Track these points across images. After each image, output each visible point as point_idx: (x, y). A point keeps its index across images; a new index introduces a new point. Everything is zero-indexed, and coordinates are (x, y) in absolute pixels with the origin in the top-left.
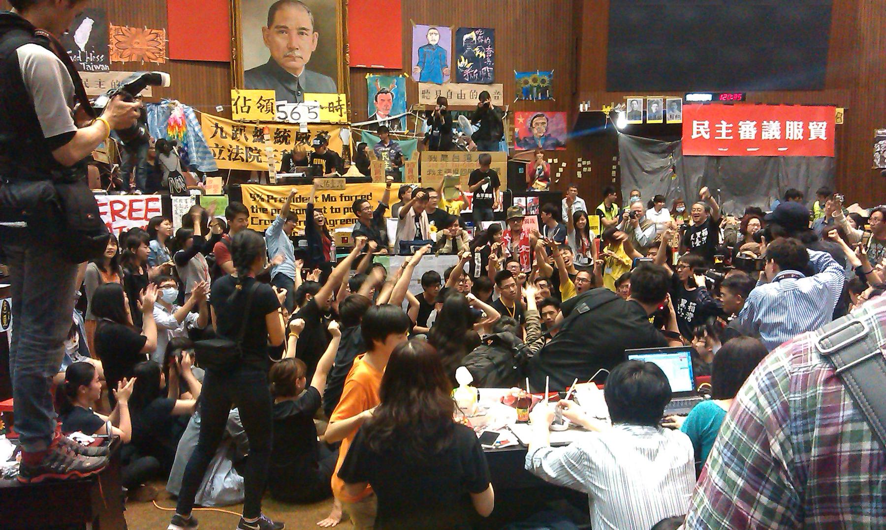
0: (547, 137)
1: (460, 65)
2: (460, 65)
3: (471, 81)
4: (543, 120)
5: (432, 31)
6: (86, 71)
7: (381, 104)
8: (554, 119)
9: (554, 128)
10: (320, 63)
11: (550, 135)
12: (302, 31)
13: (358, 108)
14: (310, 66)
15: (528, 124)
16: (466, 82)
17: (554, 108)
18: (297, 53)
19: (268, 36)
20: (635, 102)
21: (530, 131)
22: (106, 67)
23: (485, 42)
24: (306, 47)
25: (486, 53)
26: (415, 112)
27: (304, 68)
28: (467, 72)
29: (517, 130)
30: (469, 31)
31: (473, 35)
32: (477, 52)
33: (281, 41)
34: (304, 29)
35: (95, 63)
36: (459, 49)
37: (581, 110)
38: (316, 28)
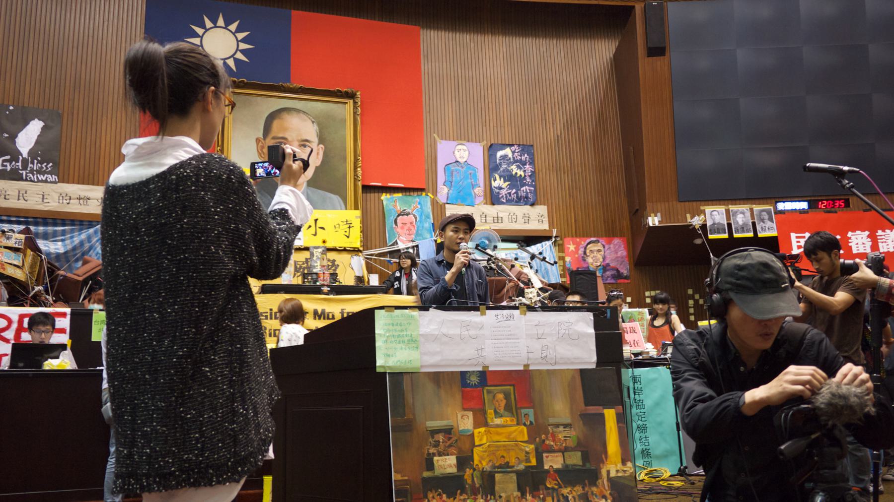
0: (605, 268)
1: (495, 184)
2: (495, 184)
3: (509, 202)
4: (599, 246)
5: (460, 147)
6: (26, 180)
7: (402, 228)
8: (612, 246)
9: (613, 256)
11: (608, 265)
13: (373, 230)
15: (581, 251)
16: (502, 203)
17: (610, 233)
20: (714, 215)
21: (585, 260)
22: (54, 178)
23: (523, 158)
25: (525, 171)
27: (305, 184)
28: (503, 192)
29: (568, 259)
30: (504, 146)
31: (508, 151)
32: (514, 169)
34: (307, 141)
35: (40, 172)
36: (492, 168)
37: (651, 225)
38: (321, 140)
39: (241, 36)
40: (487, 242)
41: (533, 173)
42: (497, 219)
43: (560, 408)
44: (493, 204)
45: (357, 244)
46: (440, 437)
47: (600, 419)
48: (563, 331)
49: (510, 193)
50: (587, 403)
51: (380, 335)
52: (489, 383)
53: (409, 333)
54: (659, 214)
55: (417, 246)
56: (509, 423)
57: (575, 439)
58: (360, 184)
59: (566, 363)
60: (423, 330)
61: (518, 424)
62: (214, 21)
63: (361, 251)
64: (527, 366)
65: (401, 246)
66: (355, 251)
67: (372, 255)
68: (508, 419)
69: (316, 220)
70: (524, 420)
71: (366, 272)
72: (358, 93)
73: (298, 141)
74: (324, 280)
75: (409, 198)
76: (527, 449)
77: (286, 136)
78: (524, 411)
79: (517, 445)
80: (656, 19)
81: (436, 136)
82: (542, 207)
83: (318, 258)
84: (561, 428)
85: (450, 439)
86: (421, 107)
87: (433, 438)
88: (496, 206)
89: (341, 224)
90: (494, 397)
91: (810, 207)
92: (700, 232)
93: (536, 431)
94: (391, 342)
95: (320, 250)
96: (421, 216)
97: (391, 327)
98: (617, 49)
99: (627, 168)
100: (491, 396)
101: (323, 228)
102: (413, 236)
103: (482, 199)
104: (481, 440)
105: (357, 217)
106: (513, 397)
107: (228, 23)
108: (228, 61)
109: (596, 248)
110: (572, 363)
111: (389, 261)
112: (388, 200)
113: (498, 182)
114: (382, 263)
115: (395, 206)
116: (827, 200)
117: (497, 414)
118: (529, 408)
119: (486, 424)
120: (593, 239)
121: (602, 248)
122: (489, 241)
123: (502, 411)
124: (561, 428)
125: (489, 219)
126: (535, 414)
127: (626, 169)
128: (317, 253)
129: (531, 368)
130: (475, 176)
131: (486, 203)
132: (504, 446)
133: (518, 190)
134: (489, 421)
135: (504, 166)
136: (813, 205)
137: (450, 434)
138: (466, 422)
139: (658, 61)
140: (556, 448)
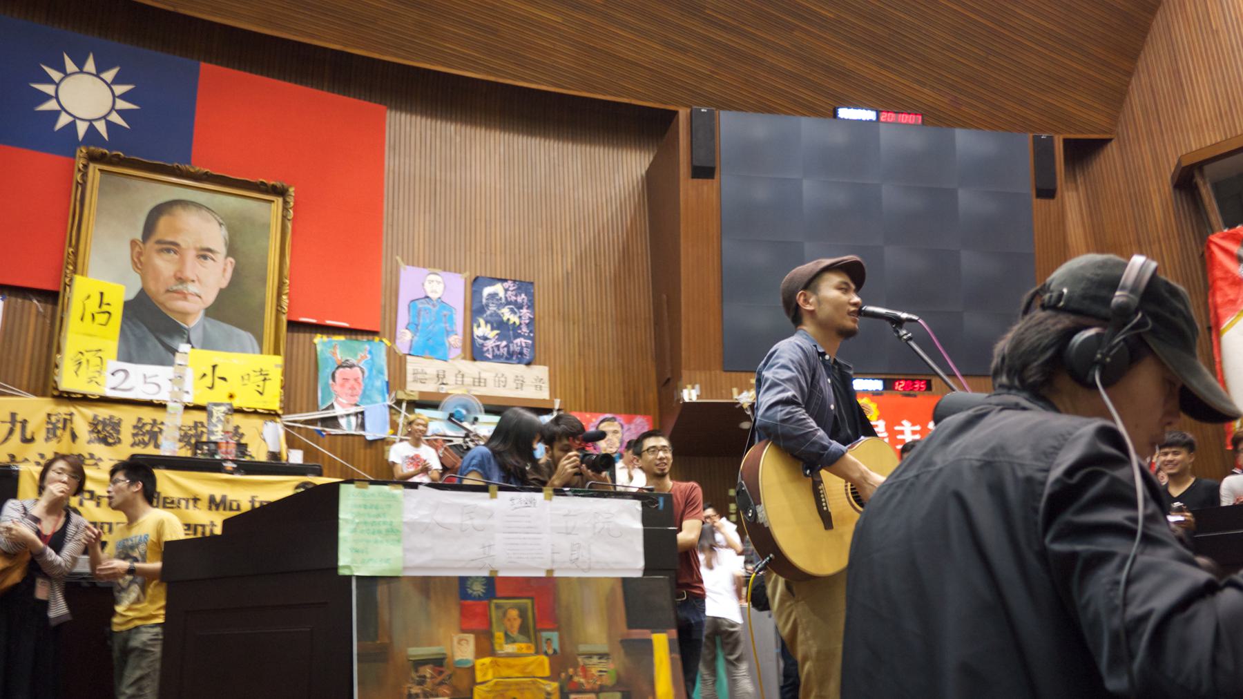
1: (478, 332)
2: (478, 332)
3: (497, 358)
4: (615, 426)
7: (342, 386)
8: (632, 426)
10: (233, 309)
12: (204, 254)
13: (299, 386)
14: (214, 312)
16: (487, 359)
18: (192, 288)
19: (140, 254)
23: (519, 300)
24: (211, 279)
26: (399, 403)
27: (201, 313)
28: (490, 344)
30: (494, 280)
31: (498, 288)
32: (506, 314)
33: (165, 265)
34: (209, 250)
37: (687, 400)
38: (231, 251)
39: (120, 89)
40: (464, 412)
41: (532, 320)
42: (479, 381)
43: (595, 632)
44: (474, 359)
45: (275, 405)
46: (427, 671)
47: (647, 647)
48: (600, 526)
49: (498, 346)
50: (632, 624)
51: (346, 521)
52: (499, 594)
53: (388, 519)
54: (697, 386)
55: (362, 413)
56: (525, 651)
57: (613, 674)
58: (284, 318)
59: (603, 570)
60: (409, 516)
61: (537, 652)
62: (80, 64)
63: (278, 415)
64: (550, 571)
65: (338, 411)
66: (271, 415)
67: (295, 422)
68: (523, 645)
69: (214, 367)
70: (545, 648)
71: (284, 446)
72: (292, 190)
73: (196, 249)
74: (227, 452)
75: (355, 344)
76: (549, 689)
77: (179, 241)
78: (545, 635)
79: (534, 683)
80: (705, 131)
81: (399, 258)
82: (541, 367)
83: (219, 420)
84: (595, 660)
85: (441, 673)
86: (382, 218)
87: (417, 671)
88: (478, 363)
89: (252, 374)
90: (505, 614)
91: (885, 388)
92: (749, 413)
93: (562, 663)
94: (362, 532)
95: (223, 409)
96: (371, 370)
97: (362, 511)
98: (651, 165)
99: (658, 323)
100: (500, 613)
101: (224, 379)
102: (358, 398)
103: (459, 351)
104: (485, 675)
105: (277, 366)
106: (530, 614)
107: (100, 69)
108: (96, 124)
109: (612, 429)
110: (612, 570)
111: (320, 432)
112: (324, 344)
113: (483, 330)
114: (309, 434)
115: (334, 353)
116: (905, 380)
117: (509, 639)
118: (552, 630)
119: (492, 652)
120: (608, 416)
121: (619, 429)
122: (468, 411)
123: (515, 633)
124: (595, 660)
125: (468, 380)
126: (561, 638)
127: (656, 324)
128: (218, 412)
129: (556, 574)
130: (452, 319)
131: (464, 358)
132: (517, 684)
133: (510, 342)
134: (497, 647)
135: (492, 308)
136: (889, 385)
137: (441, 666)
138: (464, 650)
139: (705, 185)
140: (587, 687)
